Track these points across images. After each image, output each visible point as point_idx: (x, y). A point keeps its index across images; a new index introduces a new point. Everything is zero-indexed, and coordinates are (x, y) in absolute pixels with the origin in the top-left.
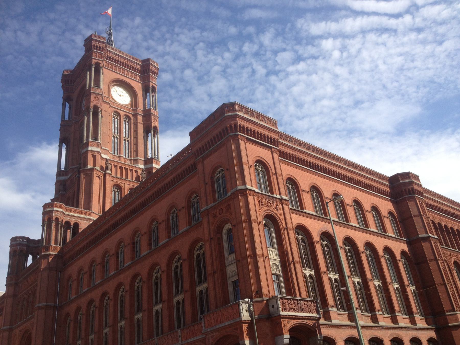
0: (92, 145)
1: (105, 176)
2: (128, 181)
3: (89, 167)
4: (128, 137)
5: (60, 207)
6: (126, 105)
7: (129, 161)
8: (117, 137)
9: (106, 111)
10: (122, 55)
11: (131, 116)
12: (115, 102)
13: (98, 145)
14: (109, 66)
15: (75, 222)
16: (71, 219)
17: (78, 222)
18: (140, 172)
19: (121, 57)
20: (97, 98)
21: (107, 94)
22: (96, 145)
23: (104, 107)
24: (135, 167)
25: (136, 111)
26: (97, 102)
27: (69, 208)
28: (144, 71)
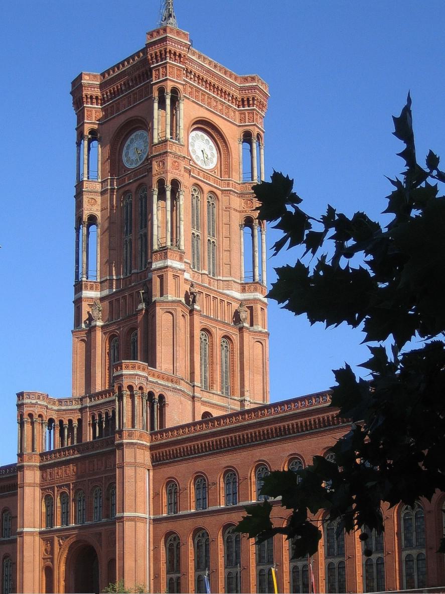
1: (191, 312)
3: (170, 298)
5: (144, 370)
11: (218, 193)
12: (195, 163)
13: (181, 259)
15: (161, 393)
17: (163, 393)
19: (208, 71)
22: (178, 258)
23: (186, 182)
24: (228, 295)
25: (228, 184)
26: (177, 171)
27: (152, 370)
28: (243, 100)
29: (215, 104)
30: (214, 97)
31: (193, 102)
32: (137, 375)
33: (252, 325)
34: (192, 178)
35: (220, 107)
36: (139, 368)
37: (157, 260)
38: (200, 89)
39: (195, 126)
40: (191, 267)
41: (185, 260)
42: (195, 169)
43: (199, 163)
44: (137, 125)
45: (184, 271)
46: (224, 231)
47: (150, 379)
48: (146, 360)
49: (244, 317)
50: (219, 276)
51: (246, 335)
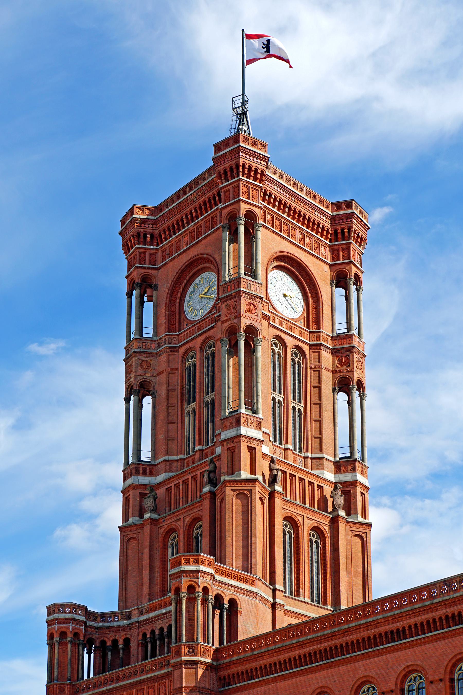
0: (247, 424)
3: (245, 474)
4: (300, 402)
5: (209, 565)
7: (303, 459)
8: (279, 400)
12: (275, 310)
13: (258, 426)
15: (231, 596)
16: (224, 590)
17: (235, 597)
18: (328, 490)
20: (252, 306)
22: (255, 424)
24: (318, 477)
26: (254, 316)
27: (220, 566)
32: (198, 571)
33: (348, 514)
36: (203, 563)
39: (276, 264)
41: (263, 429)
42: (276, 317)
44: (201, 266)
45: (262, 441)
46: (313, 396)
47: (218, 577)
48: (212, 553)
51: (342, 526)
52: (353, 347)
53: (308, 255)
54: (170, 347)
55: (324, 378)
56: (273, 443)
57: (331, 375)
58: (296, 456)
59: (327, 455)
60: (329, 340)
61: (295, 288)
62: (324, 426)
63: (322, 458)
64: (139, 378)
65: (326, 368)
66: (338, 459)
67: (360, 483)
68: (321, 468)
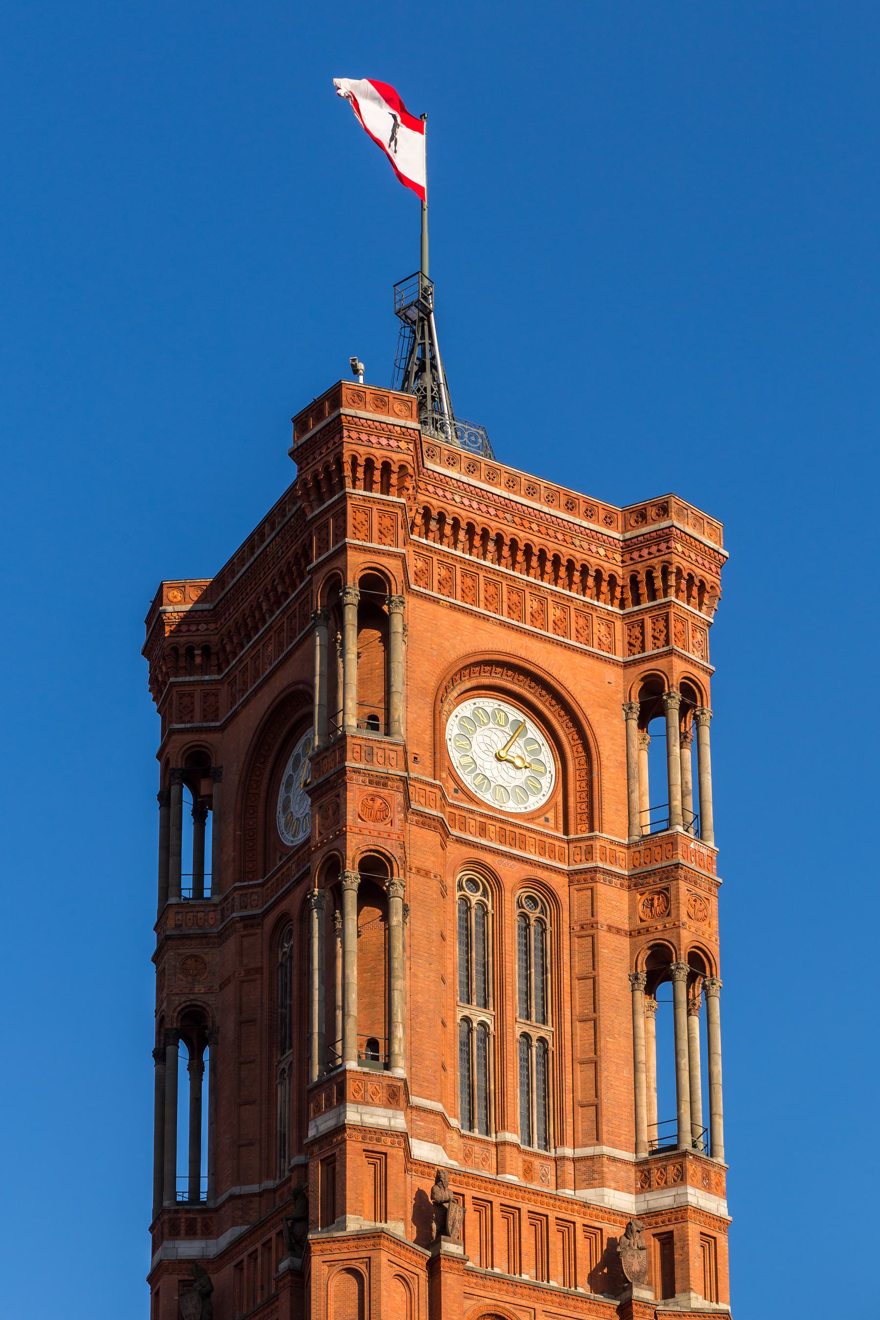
0: (363, 1097)
1: (433, 1267)
2: (551, 1291)
6: (531, 816)
7: (553, 1164)
8: (482, 1024)
9: (427, 874)
10: (505, 494)
12: (472, 798)
14: (436, 578)
21: (428, 763)
22: (383, 1095)
24: (586, 1205)
25: (590, 852)
29: (535, 605)
30: (529, 584)
31: (453, 607)
33: (669, 1291)
34: (458, 846)
35: (554, 613)
37: (318, 1111)
38: (480, 567)
40: (454, 1122)
42: (468, 815)
43: (486, 797)
46: (577, 1003)
49: (636, 1267)
50: (562, 1144)
52: (677, 866)
53: (559, 650)
54: (243, 918)
55: (604, 952)
56: (467, 1133)
57: (625, 943)
58: (532, 1159)
59: (614, 1146)
60: (622, 854)
61: (529, 735)
62: (605, 1074)
63: (601, 1156)
64: (176, 1000)
65: (610, 928)
66: (644, 1155)
67: (698, 1211)
68: (596, 1181)
